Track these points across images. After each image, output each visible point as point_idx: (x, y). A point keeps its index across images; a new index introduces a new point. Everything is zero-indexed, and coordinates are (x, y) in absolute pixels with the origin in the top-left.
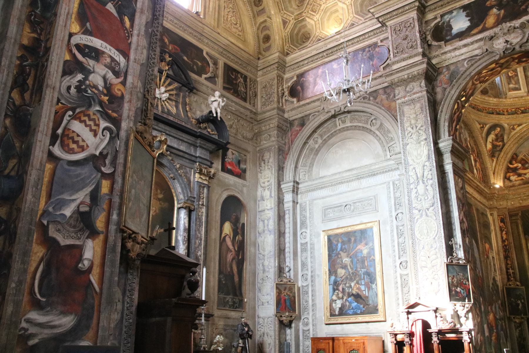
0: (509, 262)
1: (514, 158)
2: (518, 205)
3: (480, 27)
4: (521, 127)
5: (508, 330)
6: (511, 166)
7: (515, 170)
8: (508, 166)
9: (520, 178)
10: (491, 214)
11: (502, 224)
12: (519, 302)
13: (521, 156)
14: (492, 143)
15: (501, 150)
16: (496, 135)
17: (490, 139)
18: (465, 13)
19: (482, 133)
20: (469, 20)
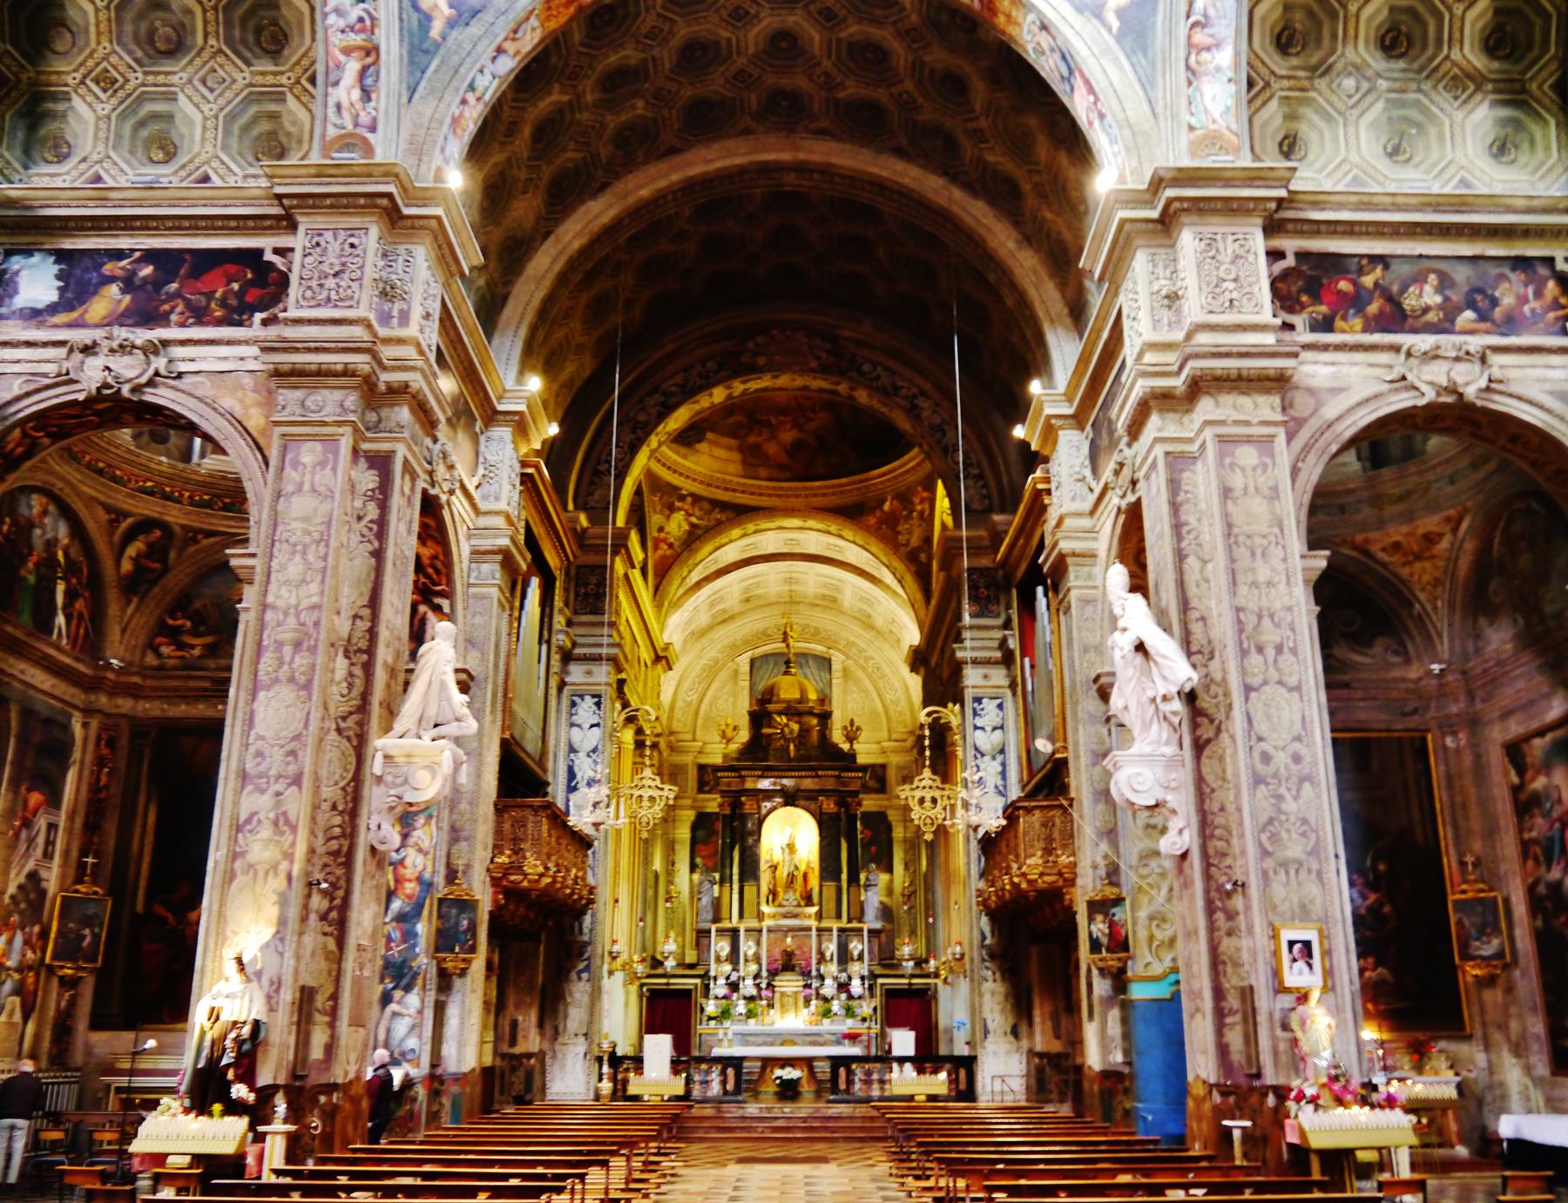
0: (96, 840)
1: (181, 605)
2: (157, 713)
3: (74, 315)
4: (212, 540)
5: (40, 993)
6: (170, 622)
7: (174, 635)
8: (164, 622)
9: (180, 653)
10: (85, 725)
11: (105, 751)
12: (87, 931)
13: (197, 604)
14: (135, 561)
15: (154, 582)
16: (150, 545)
17: (131, 551)
18: (55, 269)
19: (111, 534)
20: (59, 288)
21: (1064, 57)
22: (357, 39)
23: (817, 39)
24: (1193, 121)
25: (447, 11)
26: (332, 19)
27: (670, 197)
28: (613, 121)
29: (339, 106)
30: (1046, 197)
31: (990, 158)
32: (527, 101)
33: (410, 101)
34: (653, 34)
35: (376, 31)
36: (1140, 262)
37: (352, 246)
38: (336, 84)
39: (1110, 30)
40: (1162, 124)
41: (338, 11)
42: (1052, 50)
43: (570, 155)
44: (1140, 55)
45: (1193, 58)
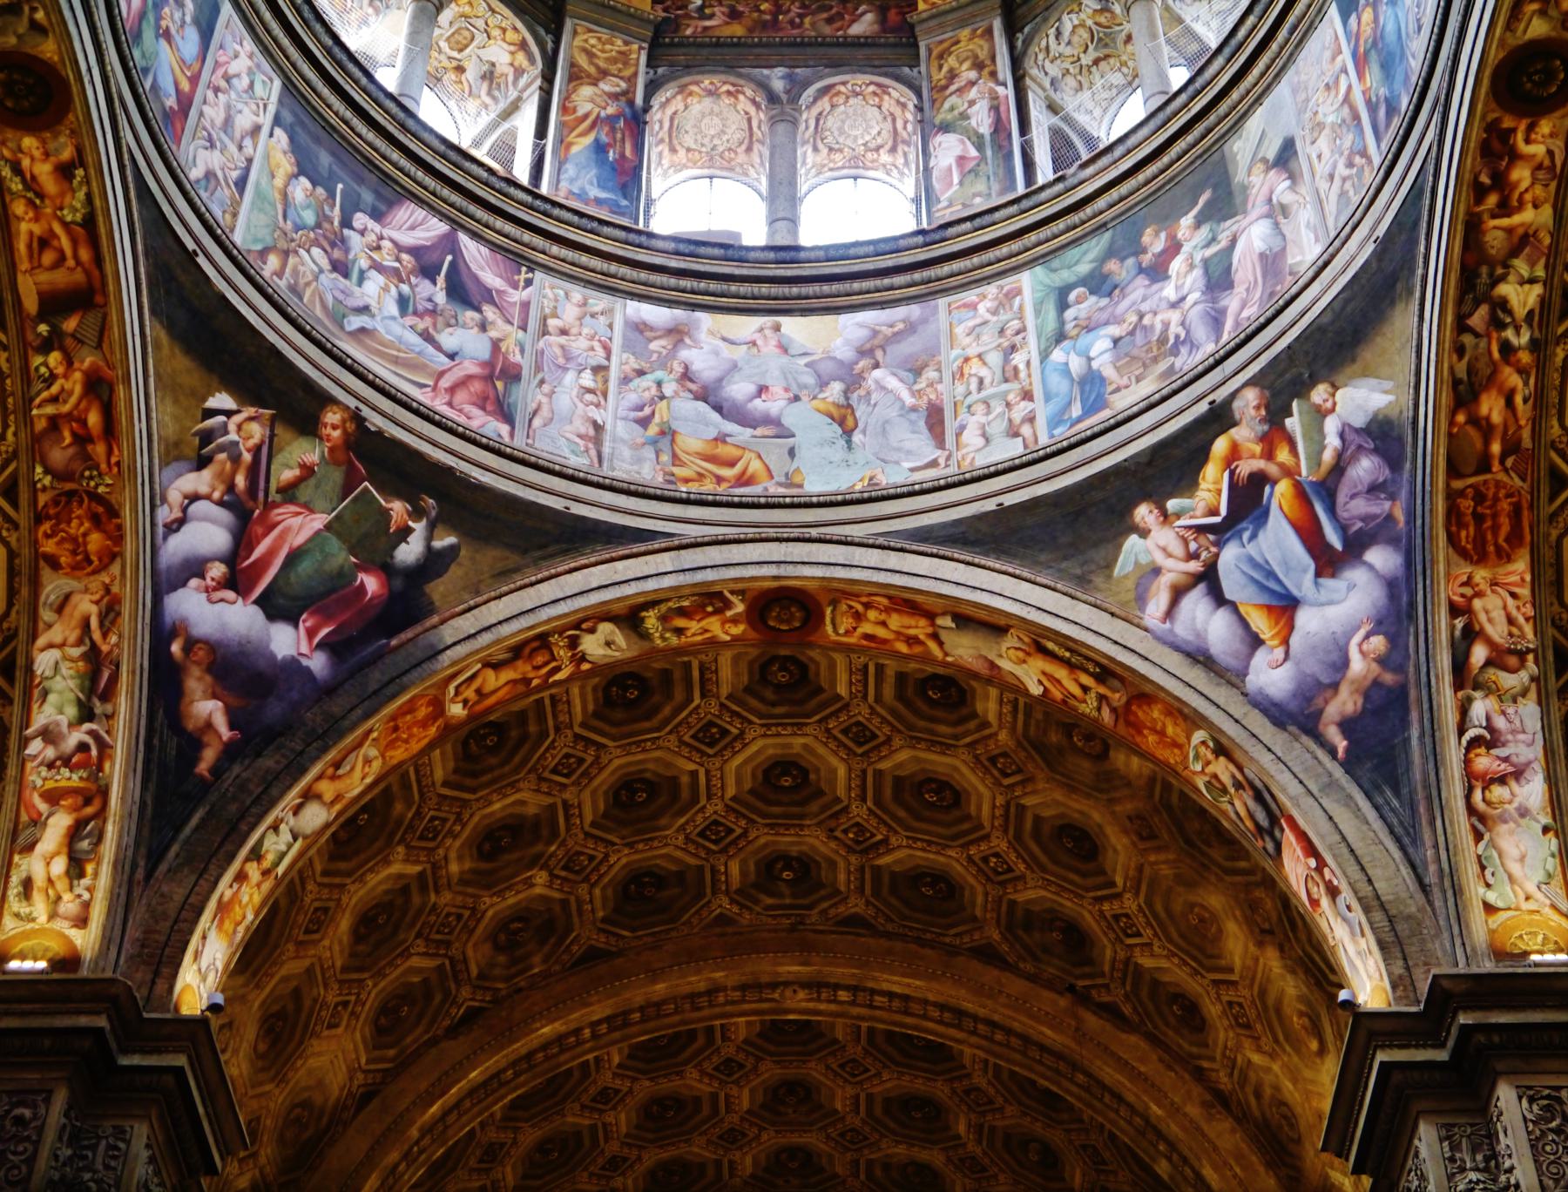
21: (1259, 797)
22: (70, 779)
23: (842, 771)
24: (1491, 897)
25: (225, 733)
26: (35, 746)
27: (587, 1032)
28: (495, 906)
29: (27, 884)
30: (1248, 1026)
31: (1147, 962)
32: (349, 874)
33: (149, 875)
34: (566, 767)
35: (107, 766)
36: (1427, 1140)
37: (19, 1120)
38: (30, 848)
39: (1332, 752)
40: (1438, 903)
41: (49, 735)
42: (1238, 786)
43: (415, 962)
44: (1389, 793)
45: (1477, 796)
